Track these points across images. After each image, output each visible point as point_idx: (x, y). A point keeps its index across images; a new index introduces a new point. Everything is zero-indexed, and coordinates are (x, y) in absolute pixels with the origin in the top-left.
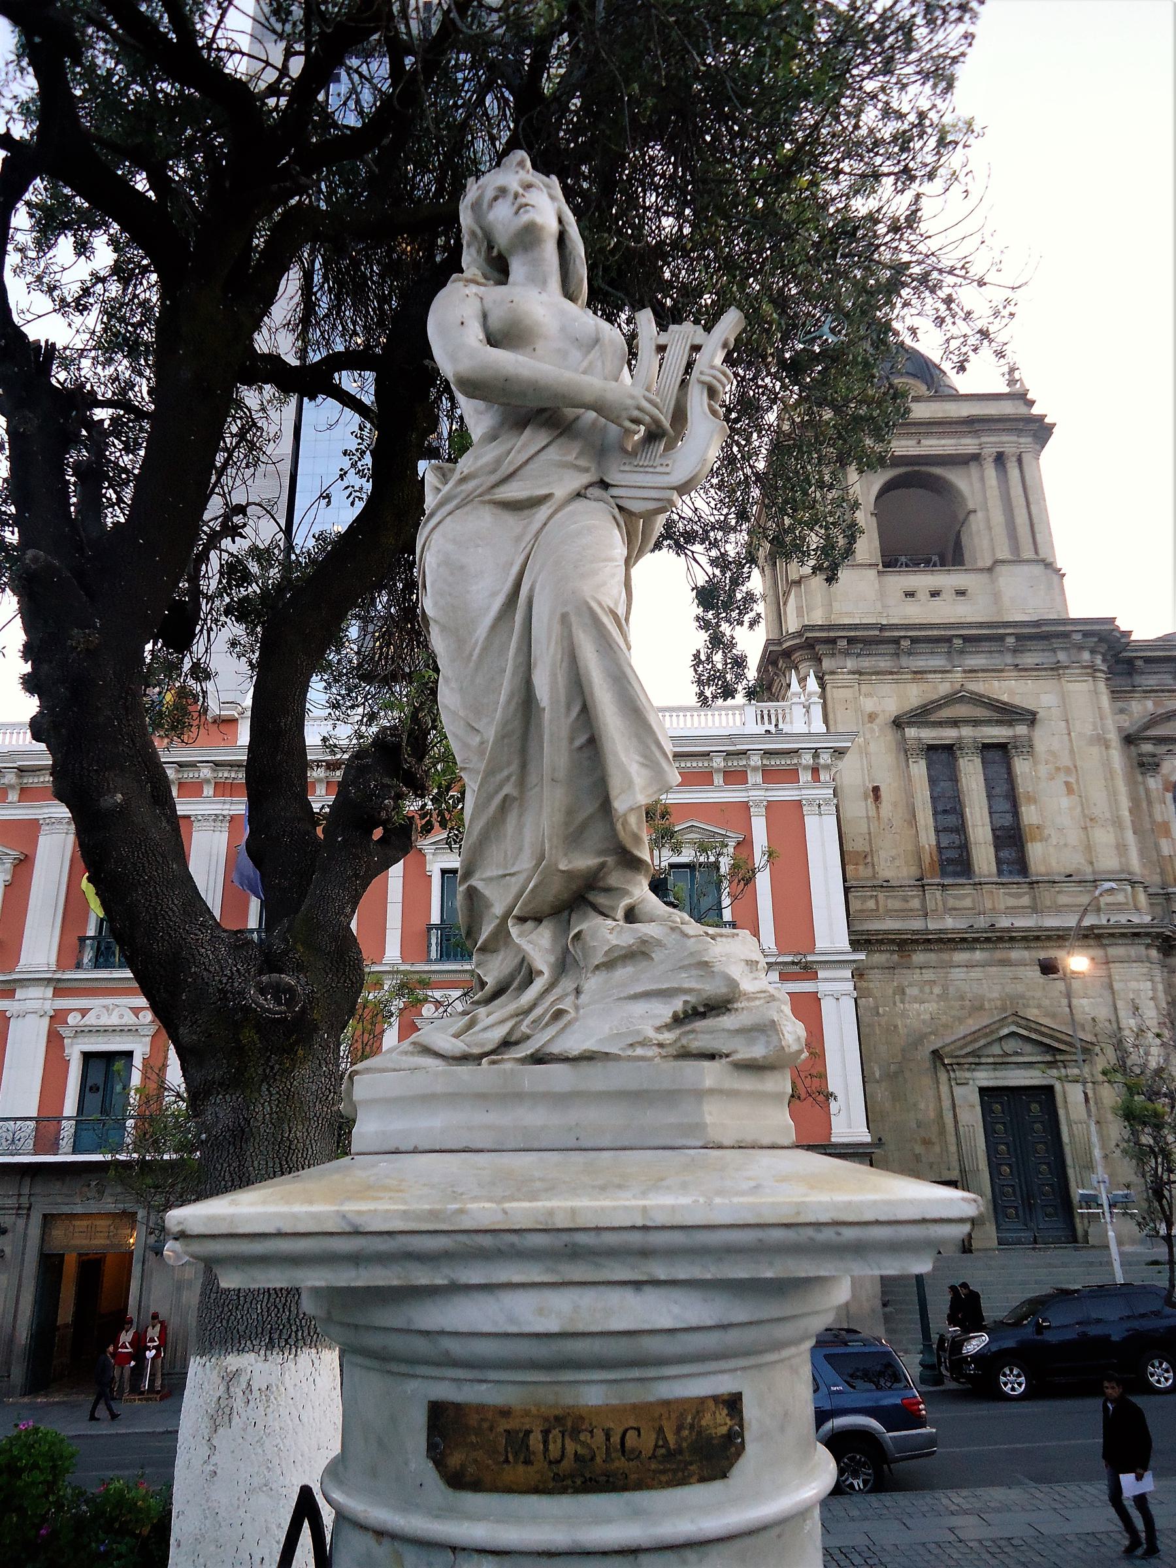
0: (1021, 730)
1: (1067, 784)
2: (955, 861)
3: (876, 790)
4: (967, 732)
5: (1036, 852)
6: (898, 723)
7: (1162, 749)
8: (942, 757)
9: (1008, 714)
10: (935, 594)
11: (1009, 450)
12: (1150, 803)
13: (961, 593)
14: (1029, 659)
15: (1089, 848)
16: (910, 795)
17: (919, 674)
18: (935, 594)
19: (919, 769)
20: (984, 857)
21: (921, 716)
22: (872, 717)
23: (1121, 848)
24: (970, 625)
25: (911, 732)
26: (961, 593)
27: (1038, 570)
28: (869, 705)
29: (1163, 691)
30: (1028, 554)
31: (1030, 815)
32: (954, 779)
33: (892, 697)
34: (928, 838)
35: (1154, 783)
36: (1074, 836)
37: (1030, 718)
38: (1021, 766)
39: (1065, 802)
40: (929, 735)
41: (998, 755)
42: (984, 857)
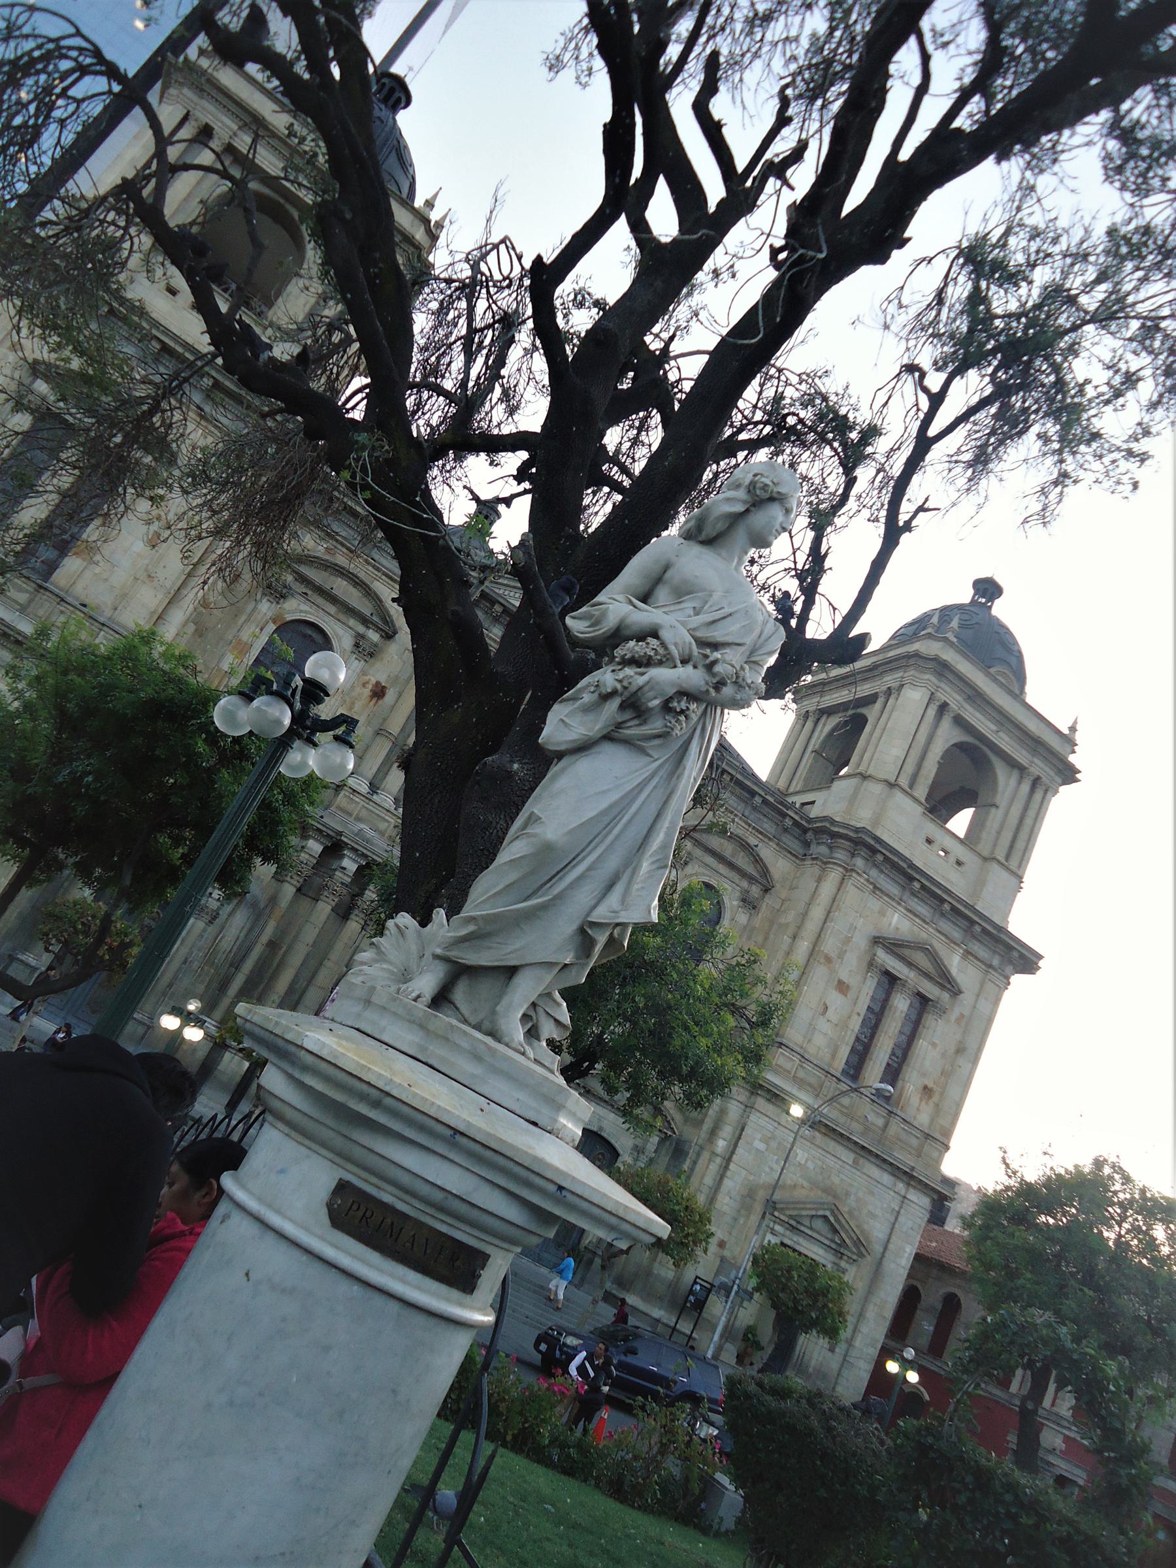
5: (71, 565)
7: (299, 588)
12: (248, 620)
15: (124, 596)
24: (175, 338)
25: (41, 387)
29: (343, 545)
35: (266, 608)
36: (120, 577)
39: (140, 547)
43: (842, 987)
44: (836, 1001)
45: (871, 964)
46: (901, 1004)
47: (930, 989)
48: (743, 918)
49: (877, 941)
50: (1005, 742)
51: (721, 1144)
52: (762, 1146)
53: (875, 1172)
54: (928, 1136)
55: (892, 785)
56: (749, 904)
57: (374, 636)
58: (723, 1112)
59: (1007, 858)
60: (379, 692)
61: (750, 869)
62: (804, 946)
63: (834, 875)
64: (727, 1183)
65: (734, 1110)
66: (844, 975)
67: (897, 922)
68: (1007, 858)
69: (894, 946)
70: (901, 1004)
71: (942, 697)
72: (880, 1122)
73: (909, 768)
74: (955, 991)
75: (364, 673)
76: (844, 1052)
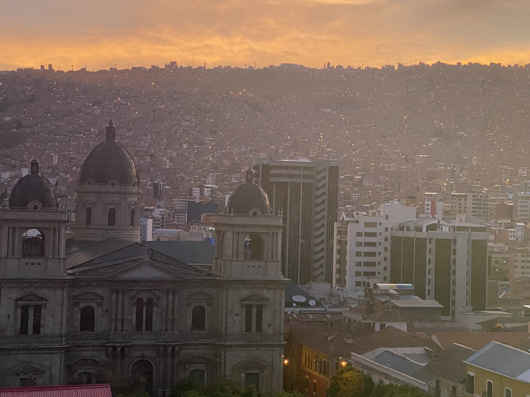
0: (44, 302)
1: (52, 315)
2: (24, 330)
3: (9, 316)
4: (31, 303)
5: (42, 329)
6: (16, 300)
8: (25, 309)
9: (41, 299)
10: (33, 264)
11: (57, 228)
13: (39, 264)
14: (50, 285)
16: (16, 317)
17: (23, 288)
18: (33, 264)
19: (19, 311)
20: (30, 331)
21: (21, 299)
22: (11, 298)
23: (61, 330)
25: (19, 302)
26: (39, 264)
27: (57, 260)
28: (10, 296)
30: (56, 256)
31: (42, 322)
32: (27, 312)
33: (15, 294)
34: (19, 326)
35: (77, 309)
37: (47, 300)
38: (43, 310)
40: (23, 303)
41: (38, 309)
42: (30, 331)
43: (237, 315)
44: (237, 319)
45: (242, 306)
46: (254, 310)
47: (259, 303)
48: (210, 308)
49: (241, 301)
50: (259, 230)
51: (223, 361)
52: (232, 357)
53: (263, 349)
54: (274, 334)
55: (232, 261)
56: (210, 304)
57: (100, 301)
58: (221, 354)
59: (272, 259)
60: (107, 311)
61: (207, 297)
62: (224, 310)
63: (225, 292)
64: (227, 368)
65: (223, 353)
66: (236, 312)
67: (245, 293)
68: (272, 259)
69: (245, 299)
70: (254, 310)
71: (236, 231)
72: (260, 338)
73: (235, 255)
74: (267, 300)
75: (102, 309)
76: (244, 328)
